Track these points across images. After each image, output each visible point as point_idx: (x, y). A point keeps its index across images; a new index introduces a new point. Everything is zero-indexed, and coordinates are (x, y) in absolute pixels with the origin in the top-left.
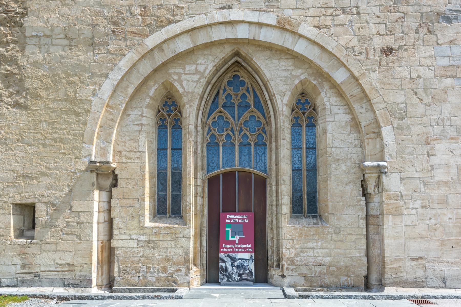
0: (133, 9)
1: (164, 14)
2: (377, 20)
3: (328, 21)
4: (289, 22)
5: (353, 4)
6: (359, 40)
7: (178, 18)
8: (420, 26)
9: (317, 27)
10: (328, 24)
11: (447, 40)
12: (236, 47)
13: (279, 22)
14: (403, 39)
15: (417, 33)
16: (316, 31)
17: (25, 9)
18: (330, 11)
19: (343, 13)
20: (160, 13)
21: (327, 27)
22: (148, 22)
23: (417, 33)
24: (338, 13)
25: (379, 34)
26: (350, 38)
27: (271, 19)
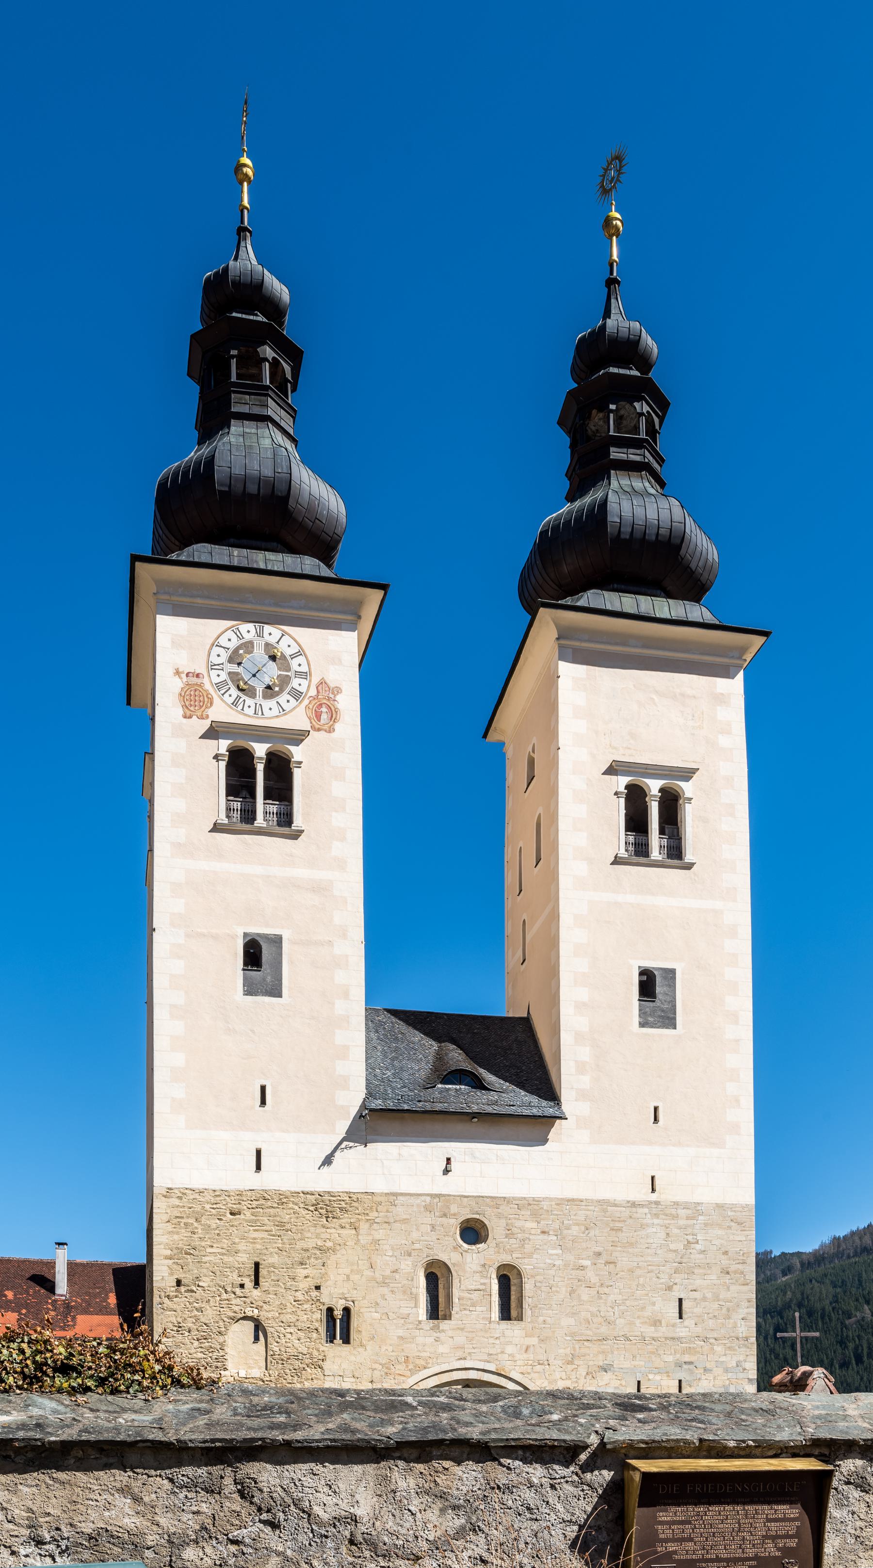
0: (399, 1359)
1: (422, 1362)
2: (561, 1369)
3: (529, 1369)
4: (503, 1370)
5: (545, 1359)
6: (549, 1383)
7: (429, 1365)
8: (587, 1374)
9: (522, 1373)
10: (529, 1371)
11: (604, 1383)
12: (467, 1383)
13: (497, 1370)
14: (576, 1382)
15: (585, 1378)
16: (521, 1376)
17: (325, 1356)
18: (530, 1362)
19: (539, 1364)
20: (418, 1362)
21: (529, 1373)
22: (410, 1368)
23: (585, 1378)
24: (536, 1364)
25: (561, 1378)
26: (543, 1381)
27: (492, 1368)
